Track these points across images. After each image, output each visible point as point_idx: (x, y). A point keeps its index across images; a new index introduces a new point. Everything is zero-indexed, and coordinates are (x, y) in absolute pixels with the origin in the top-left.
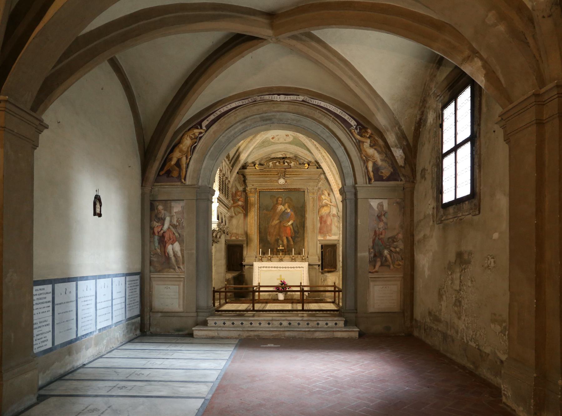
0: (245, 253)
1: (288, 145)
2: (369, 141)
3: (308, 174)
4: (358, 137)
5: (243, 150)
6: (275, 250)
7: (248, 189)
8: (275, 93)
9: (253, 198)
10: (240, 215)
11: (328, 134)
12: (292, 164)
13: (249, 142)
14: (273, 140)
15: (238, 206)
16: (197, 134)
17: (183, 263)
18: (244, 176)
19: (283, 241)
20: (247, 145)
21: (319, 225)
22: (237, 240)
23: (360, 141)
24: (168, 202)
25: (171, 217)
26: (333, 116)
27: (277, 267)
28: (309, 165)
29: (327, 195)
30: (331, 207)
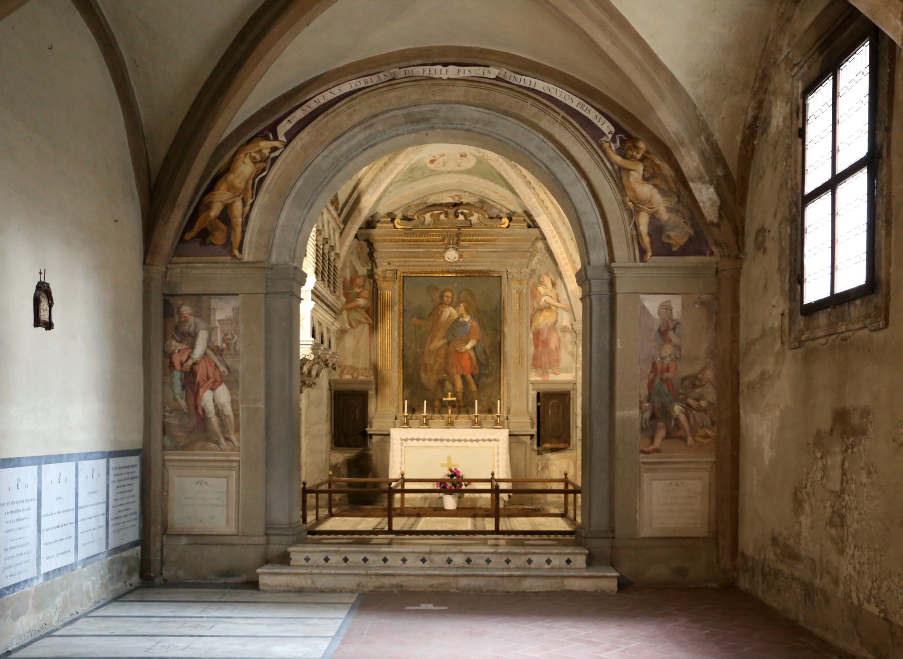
0: (372, 408)
1: (466, 176)
2: (640, 167)
3: (507, 240)
4: (618, 159)
5: (368, 186)
6: (437, 403)
7: (379, 271)
8: (437, 60)
9: (390, 292)
10: (360, 327)
11: (552, 154)
12: (474, 219)
13: (381, 169)
14: (432, 166)
15: (357, 307)
16: (266, 152)
17: (237, 430)
18: (370, 245)
19: (454, 385)
20: (376, 175)
21: (532, 349)
22: (354, 381)
23: (621, 168)
24: (205, 298)
25: (211, 331)
26: (562, 113)
27: (442, 440)
28: (510, 220)
29: (550, 285)
30: (559, 311)
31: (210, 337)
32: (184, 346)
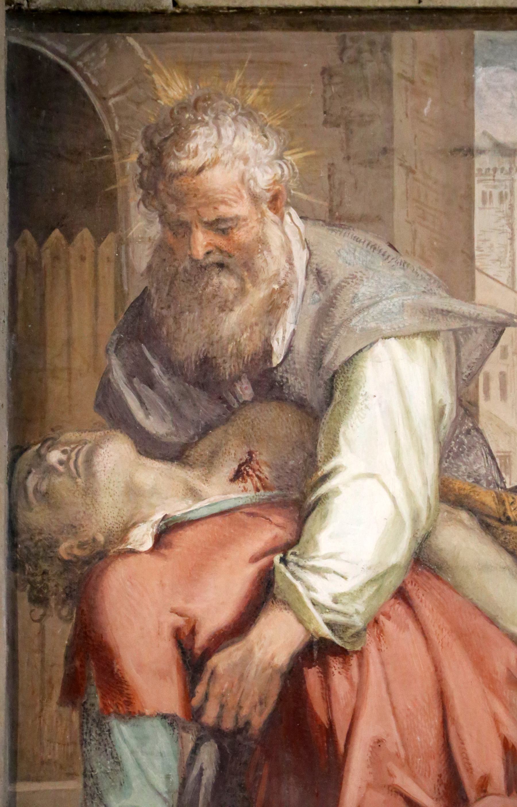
31: (467, 407)
32: (219, 492)
